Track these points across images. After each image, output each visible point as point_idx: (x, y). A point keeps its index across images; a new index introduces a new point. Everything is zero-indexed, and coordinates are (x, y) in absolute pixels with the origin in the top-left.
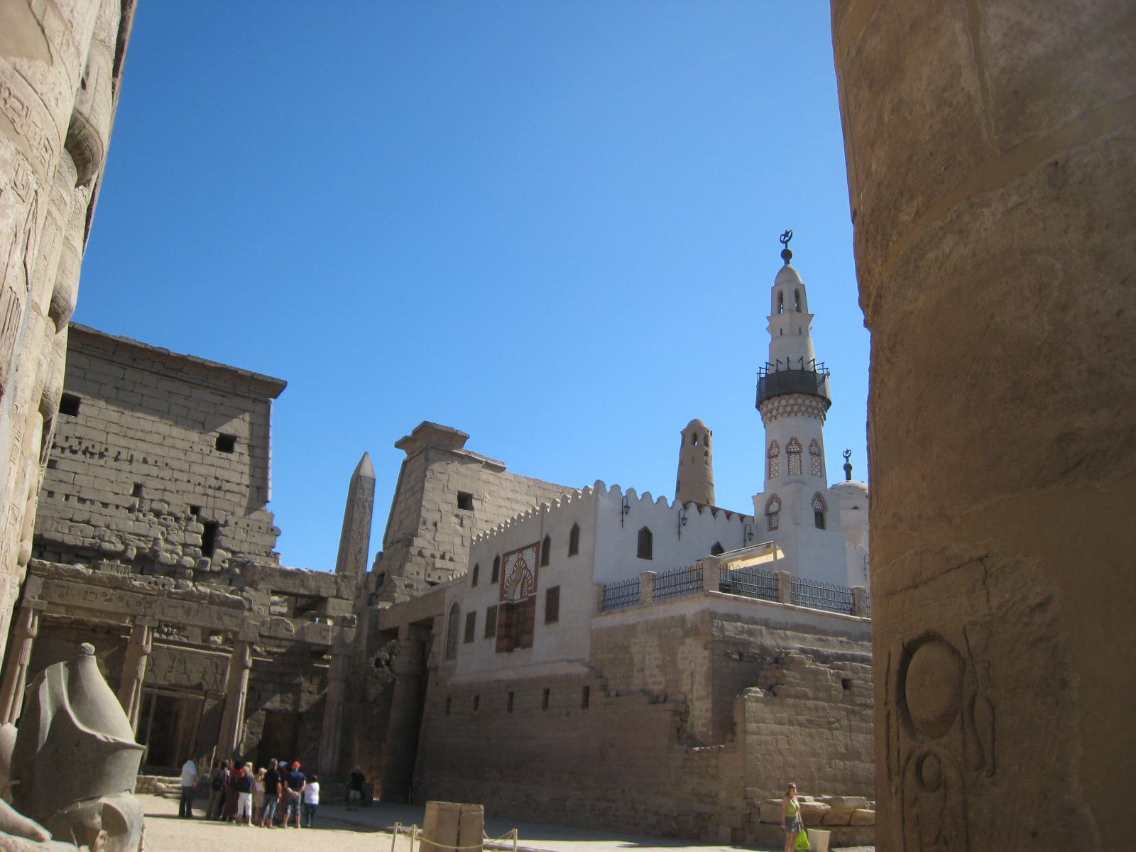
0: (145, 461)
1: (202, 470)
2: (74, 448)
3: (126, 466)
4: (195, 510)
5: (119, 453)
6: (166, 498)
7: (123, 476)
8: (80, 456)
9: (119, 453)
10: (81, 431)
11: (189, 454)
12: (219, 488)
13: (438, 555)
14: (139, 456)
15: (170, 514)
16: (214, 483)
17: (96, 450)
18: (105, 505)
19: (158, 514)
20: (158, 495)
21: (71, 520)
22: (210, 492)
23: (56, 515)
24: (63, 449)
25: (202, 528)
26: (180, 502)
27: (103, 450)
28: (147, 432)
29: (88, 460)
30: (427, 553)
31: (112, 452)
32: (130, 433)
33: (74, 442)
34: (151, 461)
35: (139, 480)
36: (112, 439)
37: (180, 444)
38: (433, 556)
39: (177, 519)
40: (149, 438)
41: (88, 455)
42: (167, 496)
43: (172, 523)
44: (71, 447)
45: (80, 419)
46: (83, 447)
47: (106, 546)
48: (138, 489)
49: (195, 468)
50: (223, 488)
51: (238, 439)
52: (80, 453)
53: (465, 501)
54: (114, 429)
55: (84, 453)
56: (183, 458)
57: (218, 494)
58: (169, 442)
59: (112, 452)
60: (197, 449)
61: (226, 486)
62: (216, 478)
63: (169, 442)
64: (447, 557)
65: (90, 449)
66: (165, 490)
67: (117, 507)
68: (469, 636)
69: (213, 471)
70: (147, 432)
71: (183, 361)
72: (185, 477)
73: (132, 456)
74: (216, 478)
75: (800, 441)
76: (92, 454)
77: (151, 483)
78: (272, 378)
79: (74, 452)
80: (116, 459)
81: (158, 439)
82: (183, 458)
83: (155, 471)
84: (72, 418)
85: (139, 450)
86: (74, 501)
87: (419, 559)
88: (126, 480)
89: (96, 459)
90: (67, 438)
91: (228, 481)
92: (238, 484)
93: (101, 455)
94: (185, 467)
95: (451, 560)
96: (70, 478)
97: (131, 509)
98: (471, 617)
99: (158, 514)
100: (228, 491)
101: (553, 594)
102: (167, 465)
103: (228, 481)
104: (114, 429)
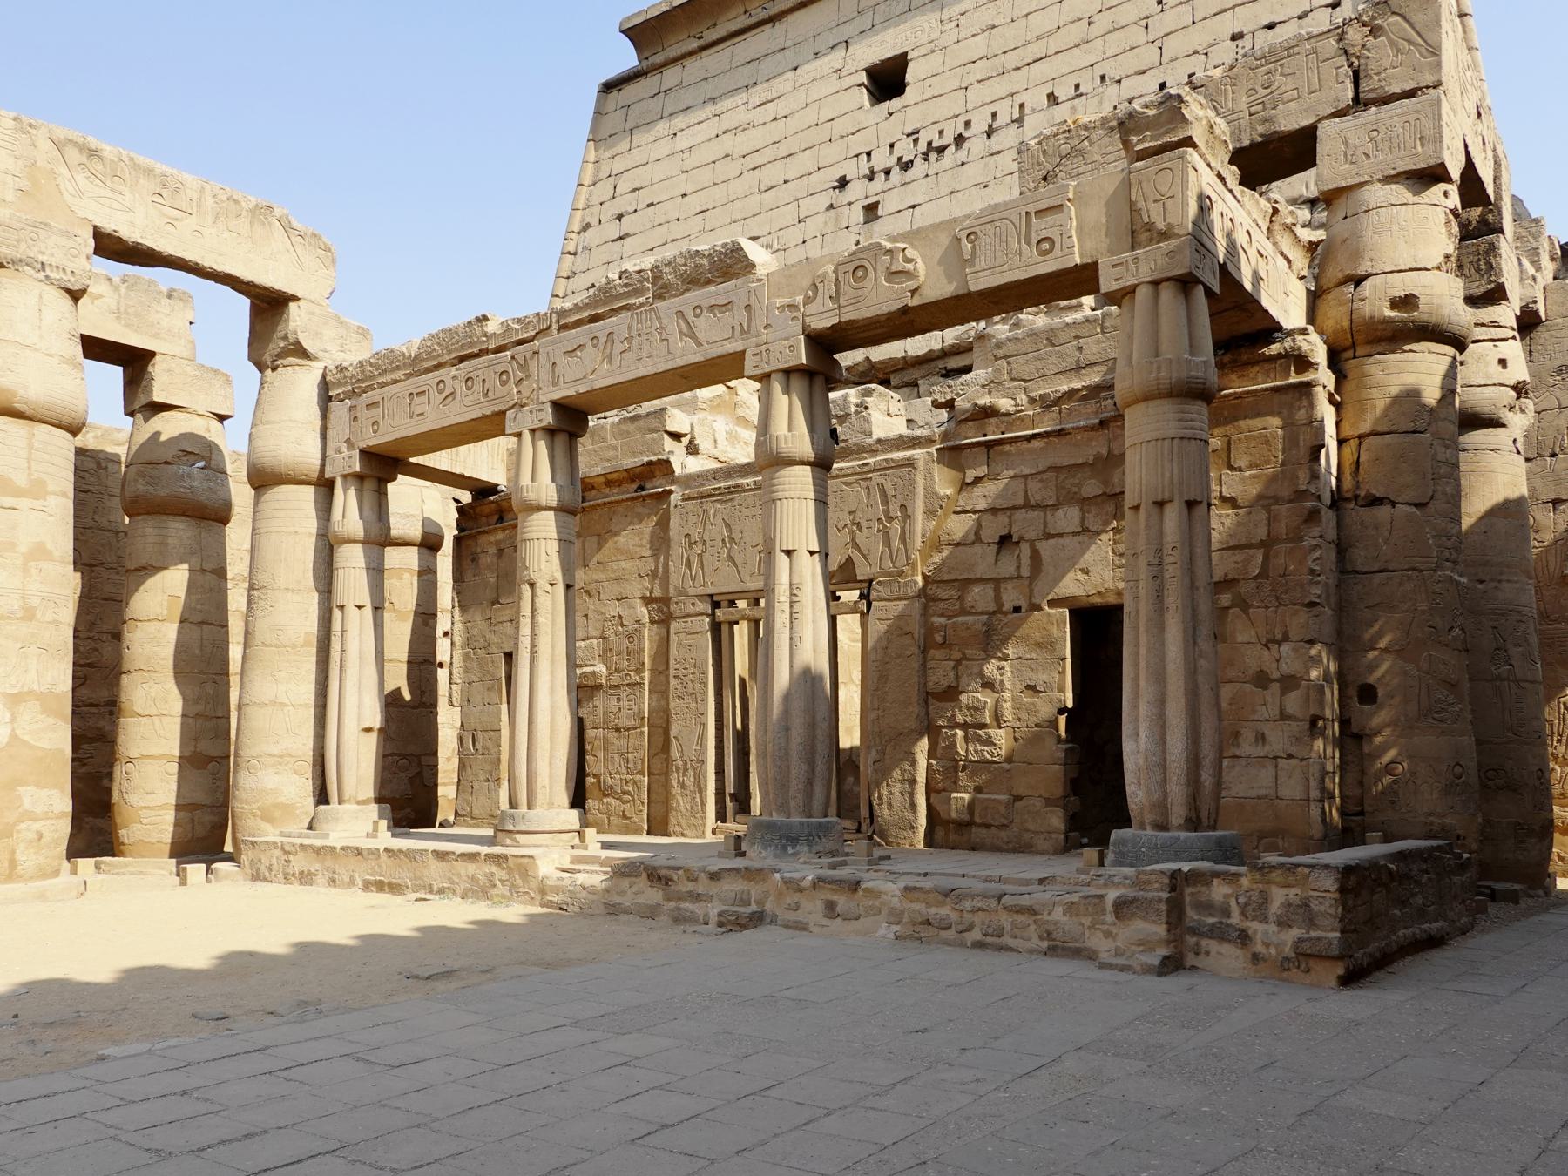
0: (1053, 99)
1: (1197, 38)
5: (994, 115)
9: (994, 115)
27: (961, 129)
28: (1050, 34)
32: (1013, 59)
33: (905, 149)
34: (1064, 92)
36: (976, 95)
40: (1054, 44)
41: (933, 156)
44: (900, 159)
45: (911, 94)
46: (922, 146)
52: (918, 162)
54: (980, 70)
56: (1139, 36)
58: (1103, 22)
59: (980, 125)
70: (1050, 34)
73: (1022, 106)
76: (941, 150)
80: (989, 133)
81: (1077, 32)
84: (896, 103)
90: (892, 146)
91: (1271, 26)
92: (1300, 18)
93: (959, 140)
94: (1150, 55)
102: (1103, 78)
103: (1271, 26)
104: (980, 70)
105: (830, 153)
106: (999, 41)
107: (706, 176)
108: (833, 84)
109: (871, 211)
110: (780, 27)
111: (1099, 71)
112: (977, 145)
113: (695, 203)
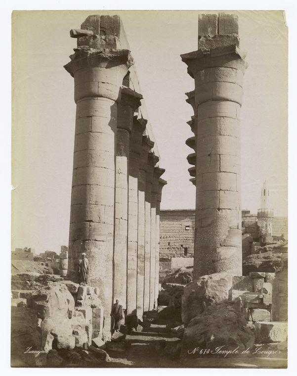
0: (170, 237)
4: (182, 246)
16: (185, 239)
18: (163, 249)
19: (174, 248)
25: (184, 249)
39: (178, 249)
43: (177, 249)
47: (164, 257)
48: (169, 243)
54: (162, 231)
71: (174, 212)
72: (179, 239)
77: (171, 242)
83: (172, 239)
99: (174, 248)
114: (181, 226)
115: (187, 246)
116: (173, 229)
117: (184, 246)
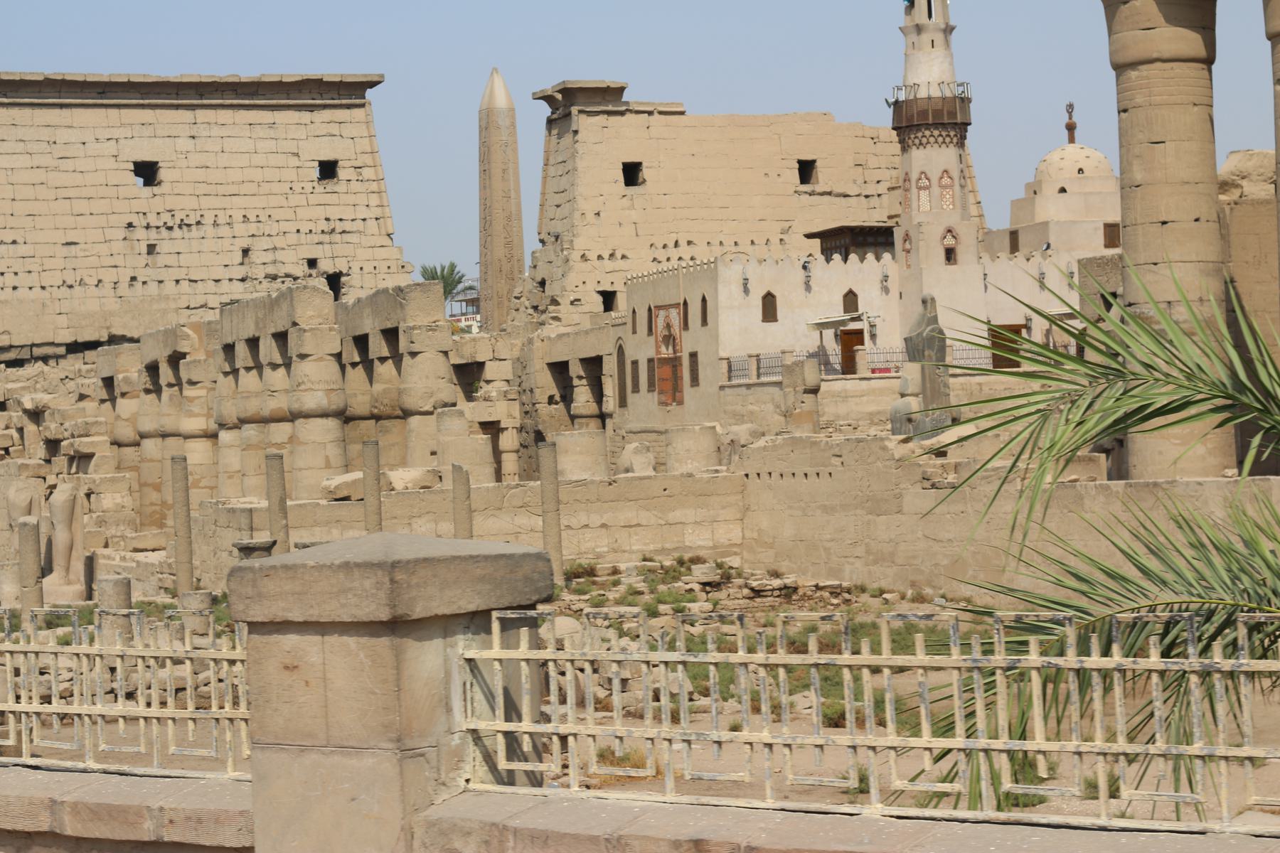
2: (170, 224)
3: (224, 231)
4: (312, 263)
6: (279, 259)
7: (226, 242)
8: (177, 233)
10: (171, 202)
11: (290, 197)
12: (333, 231)
13: (606, 256)
14: (238, 216)
15: (287, 276)
16: (324, 225)
17: (192, 221)
20: (269, 257)
21: (188, 308)
22: (326, 238)
23: (173, 305)
24: (158, 228)
26: (295, 260)
29: (187, 235)
30: (592, 255)
31: (208, 220)
32: (221, 190)
33: (166, 217)
34: (253, 218)
35: (245, 243)
36: (206, 202)
37: (276, 188)
38: (600, 257)
42: (280, 255)
48: (246, 252)
49: (302, 213)
50: (338, 230)
51: (340, 163)
52: (176, 227)
53: (632, 173)
55: (180, 227)
57: (337, 237)
60: (297, 188)
61: (339, 227)
62: (327, 219)
63: (265, 188)
64: (619, 255)
65: (186, 222)
66: (275, 248)
67: (231, 280)
68: (636, 389)
69: (321, 212)
72: (291, 227)
74: (327, 219)
75: (929, 175)
76: (189, 225)
77: (260, 245)
78: (366, 76)
79: (170, 228)
80: (215, 224)
81: (252, 188)
82: (285, 203)
84: (156, 189)
85: (237, 206)
86: (185, 284)
87: (584, 265)
88: (232, 248)
89: (195, 232)
94: (291, 215)
95: (623, 257)
96: (172, 260)
97: (243, 280)
98: (635, 363)
100: (344, 232)
101: (693, 356)
105: (121, 206)
106: (215, 176)
107: (29, 192)
108: (111, 163)
109: (151, 249)
110: (65, 112)
111: (268, 212)
112: (208, 230)
113: (20, 208)
114: (294, 161)
115: (341, 266)
116: (258, 175)
117: (326, 266)
